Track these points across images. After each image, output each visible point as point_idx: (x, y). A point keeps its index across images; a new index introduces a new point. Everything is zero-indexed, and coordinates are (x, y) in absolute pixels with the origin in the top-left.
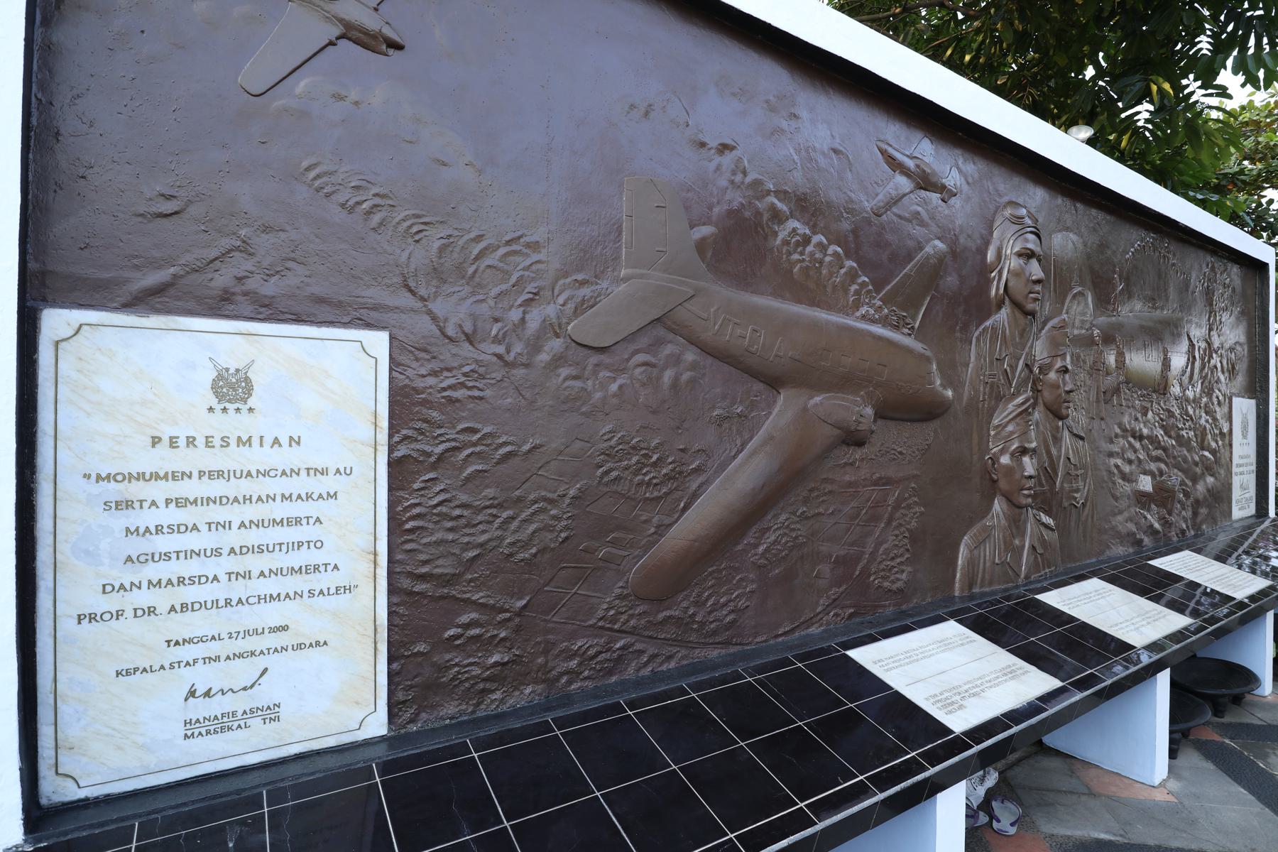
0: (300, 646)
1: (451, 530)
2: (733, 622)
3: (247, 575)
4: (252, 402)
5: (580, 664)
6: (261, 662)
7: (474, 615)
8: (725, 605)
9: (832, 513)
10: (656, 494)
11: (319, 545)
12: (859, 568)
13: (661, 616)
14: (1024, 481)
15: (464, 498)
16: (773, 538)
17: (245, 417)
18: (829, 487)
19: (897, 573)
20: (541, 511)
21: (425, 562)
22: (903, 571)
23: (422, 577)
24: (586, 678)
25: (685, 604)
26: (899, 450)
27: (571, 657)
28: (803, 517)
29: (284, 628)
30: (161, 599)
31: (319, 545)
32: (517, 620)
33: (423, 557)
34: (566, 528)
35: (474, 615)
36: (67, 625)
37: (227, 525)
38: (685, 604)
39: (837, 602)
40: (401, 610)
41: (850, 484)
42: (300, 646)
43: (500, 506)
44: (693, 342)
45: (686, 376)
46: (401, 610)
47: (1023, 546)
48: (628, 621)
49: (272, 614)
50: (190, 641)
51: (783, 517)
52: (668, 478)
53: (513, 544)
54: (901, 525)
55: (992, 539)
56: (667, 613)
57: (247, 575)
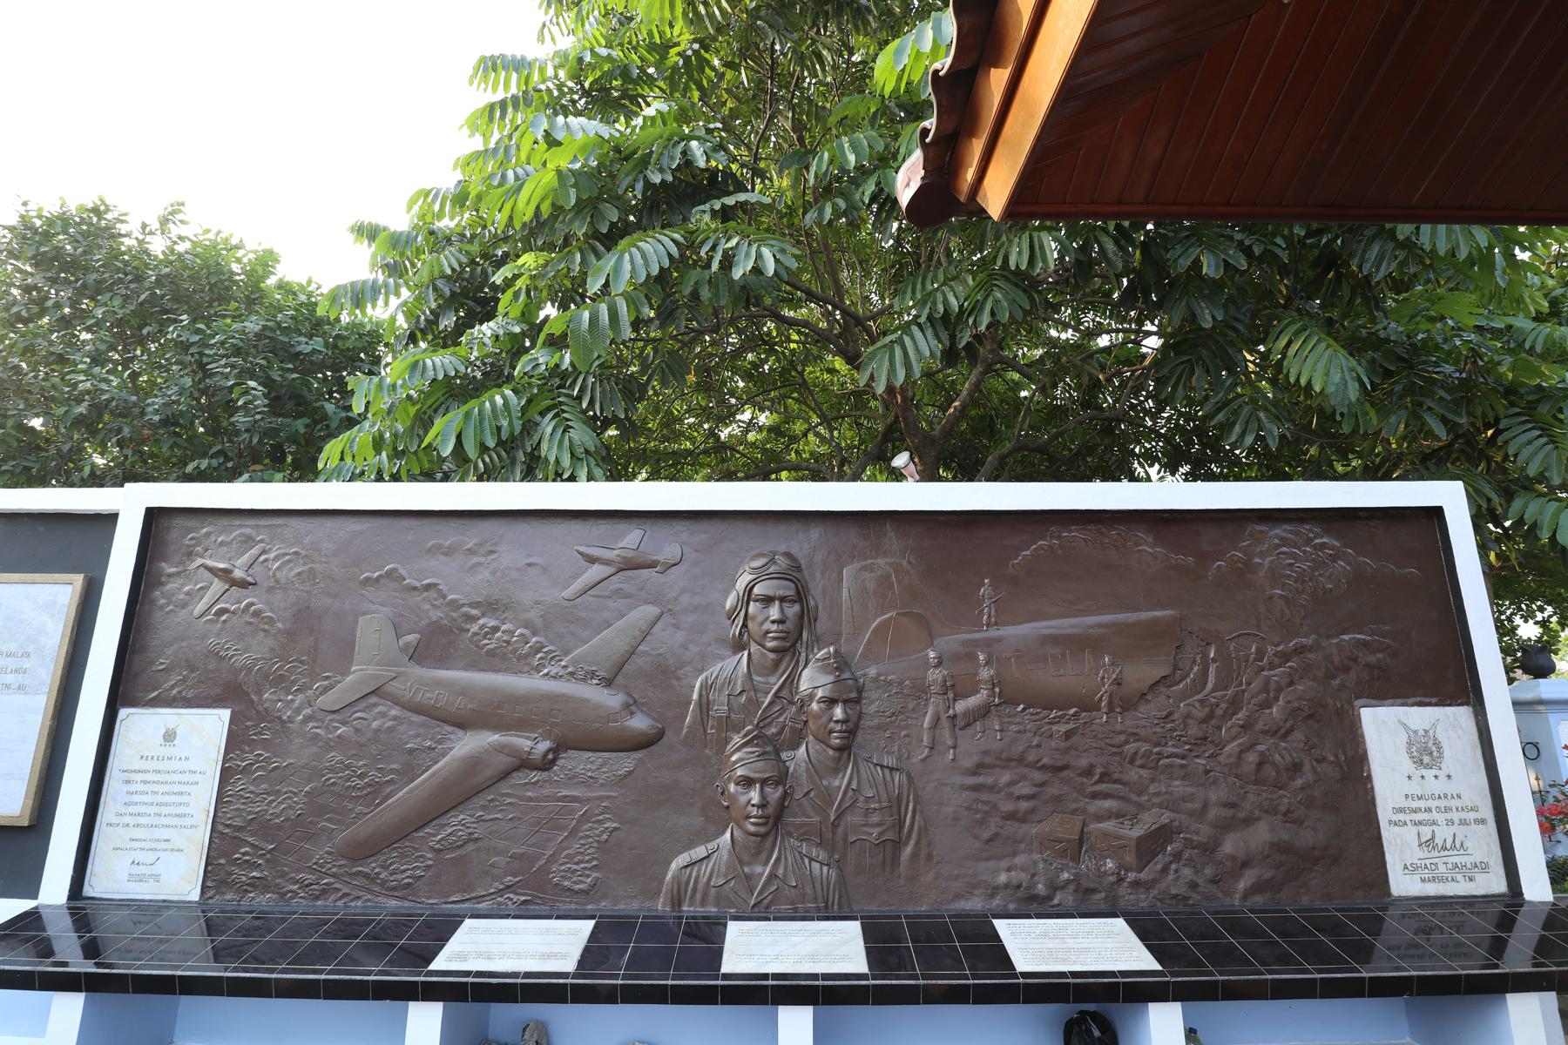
0: (173, 850)
1: (243, 803)
2: (409, 884)
3: (160, 815)
4: (175, 742)
5: (299, 888)
6: (158, 854)
7: (248, 849)
8: (405, 871)
9: (511, 819)
10: (359, 794)
11: (187, 805)
12: (537, 866)
13: (354, 870)
14: (750, 808)
15: (252, 788)
16: (449, 831)
17: (172, 748)
18: (509, 800)
19: (580, 876)
20: (289, 798)
21: (230, 819)
22: (588, 876)
23: (228, 826)
24: (301, 897)
25: (374, 865)
26: (589, 774)
27: (295, 883)
28: (480, 820)
29: (168, 841)
30: (131, 821)
31: (187, 805)
32: (268, 856)
33: (229, 816)
34: (301, 808)
35: (248, 849)
36: (104, 825)
37: (157, 793)
38: (374, 865)
39: (512, 889)
40: (217, 841)
41: (531, 799)
42: (173, 850)
43: (268, 794)
44: (397, 702)
45: (390, 723)
46: (217, 841)
47: (763, 874)
48: (330, 868)
49: (166, 833)
50: (137, 840)
51: (461, 817)
52: (368, 785)
53: (272, 814)
54: (589, 836)
55: (712, 861)
56: (360, 869)
57: (160, 815)
